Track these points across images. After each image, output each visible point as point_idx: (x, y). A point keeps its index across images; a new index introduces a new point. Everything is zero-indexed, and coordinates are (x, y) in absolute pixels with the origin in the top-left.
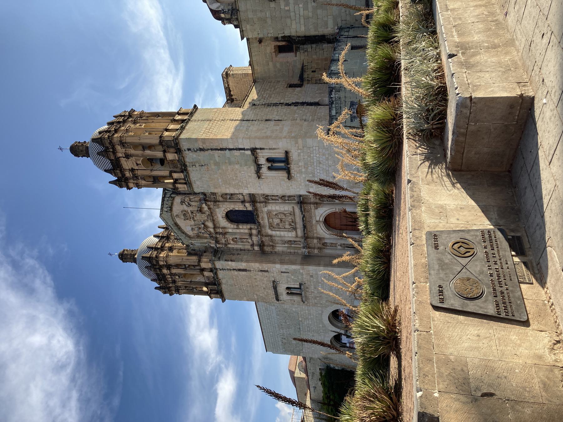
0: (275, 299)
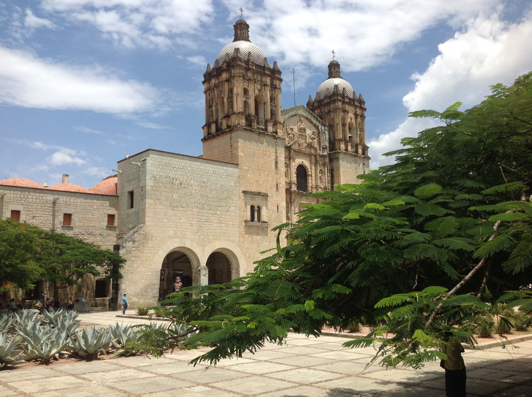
0: (244, 189)
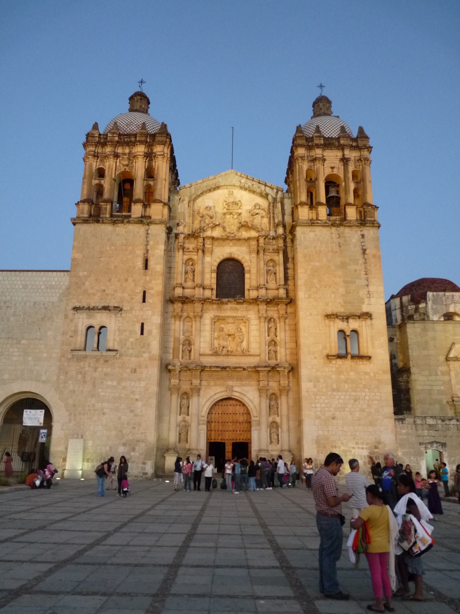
0: (77, 305)
